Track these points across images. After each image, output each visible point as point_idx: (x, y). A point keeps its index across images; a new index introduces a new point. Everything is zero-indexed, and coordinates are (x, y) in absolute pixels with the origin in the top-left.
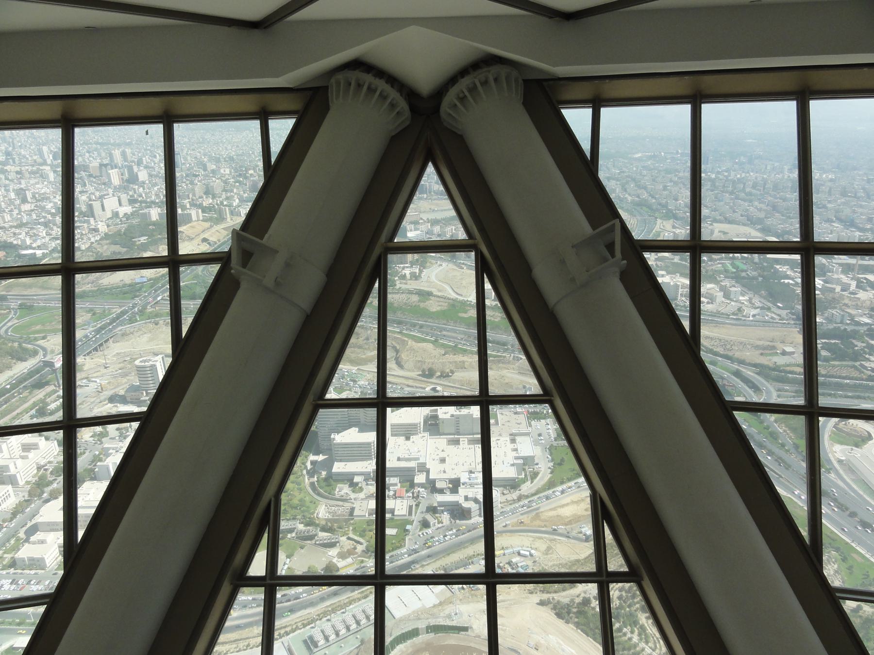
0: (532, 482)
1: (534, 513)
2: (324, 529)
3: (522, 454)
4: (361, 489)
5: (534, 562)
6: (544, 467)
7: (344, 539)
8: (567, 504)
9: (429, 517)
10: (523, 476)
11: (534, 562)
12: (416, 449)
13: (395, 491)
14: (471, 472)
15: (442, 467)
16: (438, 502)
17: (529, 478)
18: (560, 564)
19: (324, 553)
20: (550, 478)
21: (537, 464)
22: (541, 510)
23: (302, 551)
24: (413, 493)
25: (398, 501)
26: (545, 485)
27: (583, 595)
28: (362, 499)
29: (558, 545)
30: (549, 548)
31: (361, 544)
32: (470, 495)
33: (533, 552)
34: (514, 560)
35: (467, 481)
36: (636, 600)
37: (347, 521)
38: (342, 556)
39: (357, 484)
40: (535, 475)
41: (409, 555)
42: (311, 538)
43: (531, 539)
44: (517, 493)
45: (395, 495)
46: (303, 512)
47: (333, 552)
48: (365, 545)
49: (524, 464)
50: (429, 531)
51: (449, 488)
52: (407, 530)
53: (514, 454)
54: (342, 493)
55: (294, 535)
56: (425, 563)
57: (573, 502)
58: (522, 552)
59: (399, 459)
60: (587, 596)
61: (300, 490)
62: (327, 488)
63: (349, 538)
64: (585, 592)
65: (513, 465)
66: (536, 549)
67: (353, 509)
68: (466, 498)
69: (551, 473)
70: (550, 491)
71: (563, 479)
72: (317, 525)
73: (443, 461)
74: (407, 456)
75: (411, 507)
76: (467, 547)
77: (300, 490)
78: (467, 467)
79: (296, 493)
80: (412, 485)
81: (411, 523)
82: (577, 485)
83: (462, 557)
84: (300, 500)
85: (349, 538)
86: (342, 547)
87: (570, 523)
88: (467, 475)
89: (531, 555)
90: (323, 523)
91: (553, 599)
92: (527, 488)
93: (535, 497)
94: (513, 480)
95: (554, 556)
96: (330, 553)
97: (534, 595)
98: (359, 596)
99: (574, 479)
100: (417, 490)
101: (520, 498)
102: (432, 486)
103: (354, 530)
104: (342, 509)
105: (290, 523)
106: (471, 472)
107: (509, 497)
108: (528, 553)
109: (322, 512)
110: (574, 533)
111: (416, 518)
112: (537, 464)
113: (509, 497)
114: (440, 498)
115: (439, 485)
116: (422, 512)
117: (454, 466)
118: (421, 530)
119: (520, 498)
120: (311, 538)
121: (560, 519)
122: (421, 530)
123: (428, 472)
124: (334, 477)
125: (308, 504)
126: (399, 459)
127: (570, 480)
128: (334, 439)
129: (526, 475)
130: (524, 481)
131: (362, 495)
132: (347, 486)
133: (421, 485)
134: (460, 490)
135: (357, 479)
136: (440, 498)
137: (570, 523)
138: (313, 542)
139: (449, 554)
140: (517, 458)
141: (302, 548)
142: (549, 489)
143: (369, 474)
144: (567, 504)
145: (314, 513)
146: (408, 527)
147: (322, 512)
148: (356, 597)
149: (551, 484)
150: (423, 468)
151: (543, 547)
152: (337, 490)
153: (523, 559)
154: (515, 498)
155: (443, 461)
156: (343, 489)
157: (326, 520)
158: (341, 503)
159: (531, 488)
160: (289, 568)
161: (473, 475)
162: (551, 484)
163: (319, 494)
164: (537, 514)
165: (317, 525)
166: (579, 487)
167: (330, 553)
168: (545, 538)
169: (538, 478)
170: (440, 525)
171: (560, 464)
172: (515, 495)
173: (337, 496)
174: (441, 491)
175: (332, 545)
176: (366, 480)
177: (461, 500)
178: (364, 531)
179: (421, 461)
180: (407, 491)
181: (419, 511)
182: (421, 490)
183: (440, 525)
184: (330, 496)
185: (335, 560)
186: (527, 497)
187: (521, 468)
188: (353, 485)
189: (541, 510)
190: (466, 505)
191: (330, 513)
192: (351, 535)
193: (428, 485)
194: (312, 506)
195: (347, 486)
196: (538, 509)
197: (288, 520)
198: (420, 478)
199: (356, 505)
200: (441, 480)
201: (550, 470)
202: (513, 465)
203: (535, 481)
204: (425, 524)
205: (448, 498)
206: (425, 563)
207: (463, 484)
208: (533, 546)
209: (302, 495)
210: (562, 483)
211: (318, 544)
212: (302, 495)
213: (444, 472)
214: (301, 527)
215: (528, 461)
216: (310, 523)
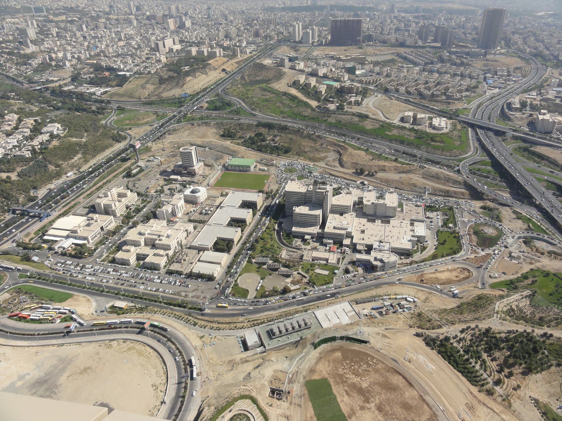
0: (421, 253)
1: (420, 274)
2: (285, 266)
3: (417, 234)
4: (309, 243)
5: (416, 306)
6: (431, 244)
7: (296, 273)
8: (444, 271)
9: (350, 268)
10: (416, 248)
11: (416, 306)
12: (346, 223)
13: (330, 248)
14: (381, 242)
15: (362, 236)
16: (357, 259)
17: (420, 250)
18: (433, 310)
19: (283, 281)
20: (434, 252)
21: (426, 242)
22: (425, 272)
23: (270, 277)
24: (341, 250)
25: (331, 254)
26: (429, 256)
27: (445, 334)
28: (309, 250)
29: (433, 297)
30: (427, 299)
31: (306, 277)
32: (378, 257)
33: (416, 299)
34: (402, 303)
35: (378, 247)
36: (482, 343)
37: (298, 262)
38: (293, 283)
39: (307, 240)
40: (424, 248)
41: (335, 289)
42: (276, 270)
43: (416, 291)
44: (410, 259)
45: (330, 249)
46: (273, 253)
47: (289, 280)
48: (308, 278)
49: (418, 241)
50: (349, 275)
51: (365, 250)
52: (335, 273)
53: (412, 233)
54: (297, 244)
55: (265, 266)
56: (344, 295)
57: (448, 270)
58: (408, 299)
59: (335, 228)
60: (448, 335)
61: (272, 239)
62: (288, 240)
63: (299, 273)
64: (447, 333)
65: (410, 241)
66: (418, 298)
67: (302, 256)
68: (376, 259)
69: (436, 249)
70: (433, 261)
71: (443, 254)
72: (280, 262)
73: (363, 232)
74: (340, 226)
75: (339, 259)
76: (372, 289)
77: (272, 239)
78: (378, 238)
79: (269, 241)
80: (341, 245)
81: (338, 269)
82: (453, 259)
83: (368, 296)
84: (271, 246)
85: (299, 273)
86: (294, 278)
87: (444, 284)
88: (378, 243)
89: (414, 302)
90: (284, 261)
91: (425, 333)
92: (417, 257)
93: (423, 264)
94: (408, 250)
95: (430, 304)
96: (286, 281)
97: (413, 328)
98: (302, 309)
99: (452, 255)
100: (344, 248)
101: (411, 263)
102: (354, 248)
103: (302, 268)
104: (296, 255)
105: (264, 259)
106: (381, 242)
107: (405, 261)
108: (412, 300)
109: (284, 254)
110: (445, 291)
111: (342, 266)
112: (426, 242)
113: (405, 261)
114: (358, 256)
115: (358, 247)
116: (346, 264)
117: (370, 237)
118: (344, 274)
119: (411, 263)
120: (276, 270)
121: (438, 281)
122: (344, 274)
123: (352, 238)
124: (293, 234)
125: (276, 248)
126: (335, 228)
127: (448, 255)
128: (295, 210)
129: (417, 248)
130: (416, 252)
131: (309, 247)
132: (300, 240)
133: (347, 246)
134: (372, 252)
135: (307, 237)
136: (358, 256)
137: (444, 284)
138: (277, 272)
139: (360, 292)
140: (413, 236)
141: (270, 275)
142: (432, 260)
143: (314, 234)
144: (444, 271)
145: (278, 255)
146: (336, 271)
147: (284, 254)
148: (300, 309)
149: (434, 257)
150: (349, 236)
151: (423, 297)
152: (294, 242)
153: (408, 303)
154: (408, 262)
155: (363, 232)
156: (298, 242)
157: (286, 259)
158: (296, 250)
159: (420, 257)
160: (262, 286)
161: (382, 244)
162: (434, 257)
163: (283, 243)
164: (422, 275)
165: (280, 262)
166: (454, 261)
167: (286, 281)
168: (425, 291)
169: (426, 251)
170: (356, 273)
171: (442, 244)
172: (408, 261)
173: (294, 246)
174: (360, 252)
175: (288, 276)
176: (312, 238)
177: (372, 260)
178: (308, 270)
179: (349, 230)
180: (338, 248)
181: (344, 262)
182: (347, 249)
183: (356, 273)
184: (289, 245)
185: (289, 285)
186: (417, 262)
187: (414, 243)
188: (304, 241)
189: (425, 272)
190: (375, 263)
191: (288, 255)
192: (300, 271)
193: (351, 247)
194: (278, 249)
195: (300, 240)
196: (423, 271)
197: (263, 257)
198: (347, 242)
199: (305, 253)
200: (360, 244)
201: (435, 247)
202: (410, 241)
203: (424, 253)
204: (347, 271)
205: (364, 257)
206: (344, 295)
207: (375, 249)
208: (416, 296)
209: (273, 243)
210: (443, 256)
211: (281, 275)
212: (273, 243)
213: (363, 239)
214: (270, 262)
215: (420, 241)
216: (276, 260)
